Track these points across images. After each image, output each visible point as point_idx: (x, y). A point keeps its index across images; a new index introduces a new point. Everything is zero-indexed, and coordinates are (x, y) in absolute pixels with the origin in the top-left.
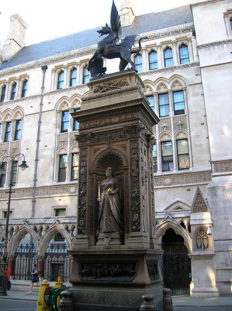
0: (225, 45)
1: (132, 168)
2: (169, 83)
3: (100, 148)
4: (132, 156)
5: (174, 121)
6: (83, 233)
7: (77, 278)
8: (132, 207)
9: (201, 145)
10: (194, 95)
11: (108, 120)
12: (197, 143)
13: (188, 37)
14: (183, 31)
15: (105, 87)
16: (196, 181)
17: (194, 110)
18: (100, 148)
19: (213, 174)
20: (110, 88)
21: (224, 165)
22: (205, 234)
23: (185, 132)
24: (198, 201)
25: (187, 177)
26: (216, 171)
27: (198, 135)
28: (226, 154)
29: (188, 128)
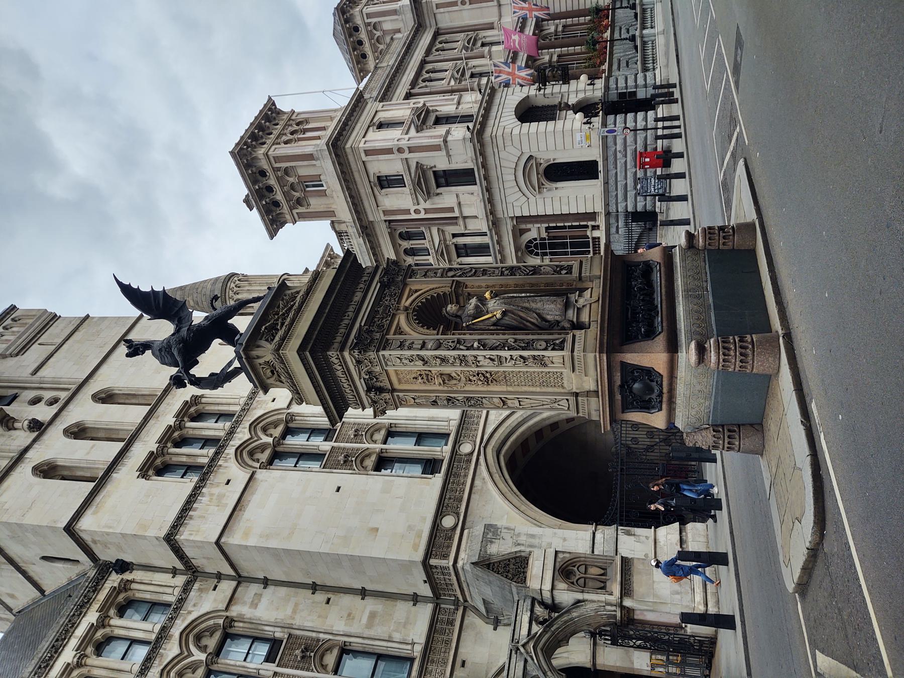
0: (204, 490)
1: (459, 274)
2: (190, 654)
3: (398, 324)
4: (438, 275)
5: (286, 666)
6: (563, 342)
7: (660, 341)
8: (528, 274)
9: (373, 615)
10: (254, 605)
11: (351, 309)
12: (364, 620)
13: (116, 584)
14: (94, 592)
15: (277, 320)
16: (448, 642)
17: (289, 611)
18: (398, 324)
19: (451, 563)
20: (283, 314)
21: (440, 540)
22: (575, 569)
23: (325, 646)
24: (501, 570)
25: (433, 661)
26: (445, 556)
27: (349, 615)
28: (419, 536)
29: (322, 636)
